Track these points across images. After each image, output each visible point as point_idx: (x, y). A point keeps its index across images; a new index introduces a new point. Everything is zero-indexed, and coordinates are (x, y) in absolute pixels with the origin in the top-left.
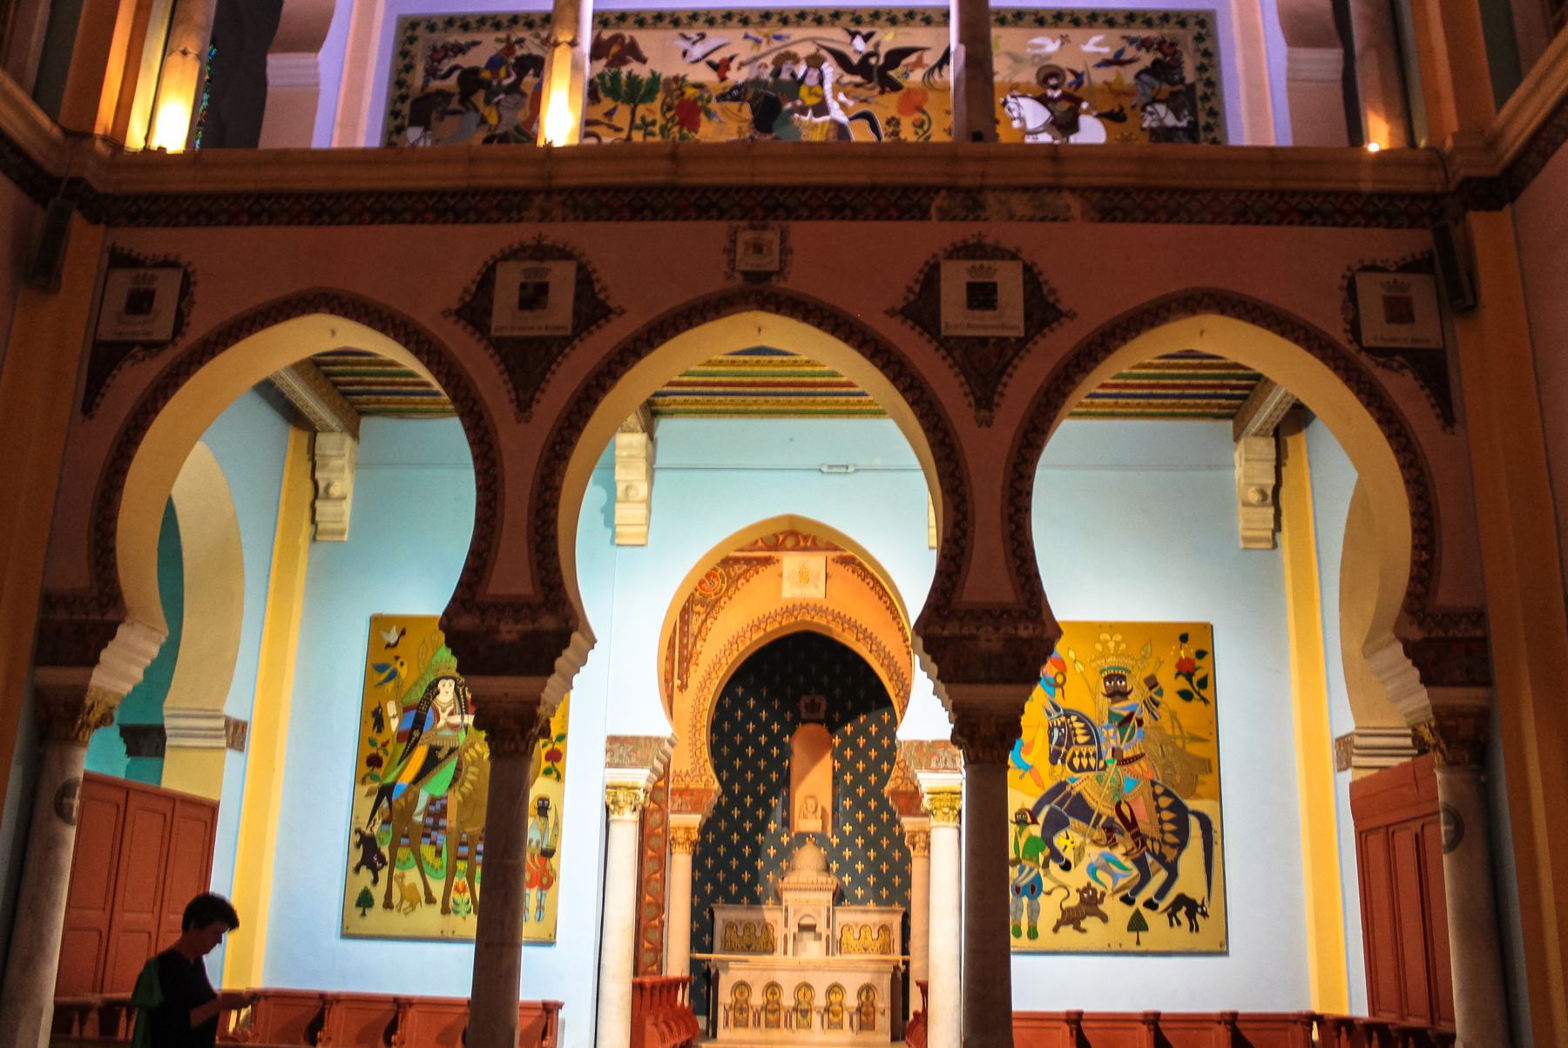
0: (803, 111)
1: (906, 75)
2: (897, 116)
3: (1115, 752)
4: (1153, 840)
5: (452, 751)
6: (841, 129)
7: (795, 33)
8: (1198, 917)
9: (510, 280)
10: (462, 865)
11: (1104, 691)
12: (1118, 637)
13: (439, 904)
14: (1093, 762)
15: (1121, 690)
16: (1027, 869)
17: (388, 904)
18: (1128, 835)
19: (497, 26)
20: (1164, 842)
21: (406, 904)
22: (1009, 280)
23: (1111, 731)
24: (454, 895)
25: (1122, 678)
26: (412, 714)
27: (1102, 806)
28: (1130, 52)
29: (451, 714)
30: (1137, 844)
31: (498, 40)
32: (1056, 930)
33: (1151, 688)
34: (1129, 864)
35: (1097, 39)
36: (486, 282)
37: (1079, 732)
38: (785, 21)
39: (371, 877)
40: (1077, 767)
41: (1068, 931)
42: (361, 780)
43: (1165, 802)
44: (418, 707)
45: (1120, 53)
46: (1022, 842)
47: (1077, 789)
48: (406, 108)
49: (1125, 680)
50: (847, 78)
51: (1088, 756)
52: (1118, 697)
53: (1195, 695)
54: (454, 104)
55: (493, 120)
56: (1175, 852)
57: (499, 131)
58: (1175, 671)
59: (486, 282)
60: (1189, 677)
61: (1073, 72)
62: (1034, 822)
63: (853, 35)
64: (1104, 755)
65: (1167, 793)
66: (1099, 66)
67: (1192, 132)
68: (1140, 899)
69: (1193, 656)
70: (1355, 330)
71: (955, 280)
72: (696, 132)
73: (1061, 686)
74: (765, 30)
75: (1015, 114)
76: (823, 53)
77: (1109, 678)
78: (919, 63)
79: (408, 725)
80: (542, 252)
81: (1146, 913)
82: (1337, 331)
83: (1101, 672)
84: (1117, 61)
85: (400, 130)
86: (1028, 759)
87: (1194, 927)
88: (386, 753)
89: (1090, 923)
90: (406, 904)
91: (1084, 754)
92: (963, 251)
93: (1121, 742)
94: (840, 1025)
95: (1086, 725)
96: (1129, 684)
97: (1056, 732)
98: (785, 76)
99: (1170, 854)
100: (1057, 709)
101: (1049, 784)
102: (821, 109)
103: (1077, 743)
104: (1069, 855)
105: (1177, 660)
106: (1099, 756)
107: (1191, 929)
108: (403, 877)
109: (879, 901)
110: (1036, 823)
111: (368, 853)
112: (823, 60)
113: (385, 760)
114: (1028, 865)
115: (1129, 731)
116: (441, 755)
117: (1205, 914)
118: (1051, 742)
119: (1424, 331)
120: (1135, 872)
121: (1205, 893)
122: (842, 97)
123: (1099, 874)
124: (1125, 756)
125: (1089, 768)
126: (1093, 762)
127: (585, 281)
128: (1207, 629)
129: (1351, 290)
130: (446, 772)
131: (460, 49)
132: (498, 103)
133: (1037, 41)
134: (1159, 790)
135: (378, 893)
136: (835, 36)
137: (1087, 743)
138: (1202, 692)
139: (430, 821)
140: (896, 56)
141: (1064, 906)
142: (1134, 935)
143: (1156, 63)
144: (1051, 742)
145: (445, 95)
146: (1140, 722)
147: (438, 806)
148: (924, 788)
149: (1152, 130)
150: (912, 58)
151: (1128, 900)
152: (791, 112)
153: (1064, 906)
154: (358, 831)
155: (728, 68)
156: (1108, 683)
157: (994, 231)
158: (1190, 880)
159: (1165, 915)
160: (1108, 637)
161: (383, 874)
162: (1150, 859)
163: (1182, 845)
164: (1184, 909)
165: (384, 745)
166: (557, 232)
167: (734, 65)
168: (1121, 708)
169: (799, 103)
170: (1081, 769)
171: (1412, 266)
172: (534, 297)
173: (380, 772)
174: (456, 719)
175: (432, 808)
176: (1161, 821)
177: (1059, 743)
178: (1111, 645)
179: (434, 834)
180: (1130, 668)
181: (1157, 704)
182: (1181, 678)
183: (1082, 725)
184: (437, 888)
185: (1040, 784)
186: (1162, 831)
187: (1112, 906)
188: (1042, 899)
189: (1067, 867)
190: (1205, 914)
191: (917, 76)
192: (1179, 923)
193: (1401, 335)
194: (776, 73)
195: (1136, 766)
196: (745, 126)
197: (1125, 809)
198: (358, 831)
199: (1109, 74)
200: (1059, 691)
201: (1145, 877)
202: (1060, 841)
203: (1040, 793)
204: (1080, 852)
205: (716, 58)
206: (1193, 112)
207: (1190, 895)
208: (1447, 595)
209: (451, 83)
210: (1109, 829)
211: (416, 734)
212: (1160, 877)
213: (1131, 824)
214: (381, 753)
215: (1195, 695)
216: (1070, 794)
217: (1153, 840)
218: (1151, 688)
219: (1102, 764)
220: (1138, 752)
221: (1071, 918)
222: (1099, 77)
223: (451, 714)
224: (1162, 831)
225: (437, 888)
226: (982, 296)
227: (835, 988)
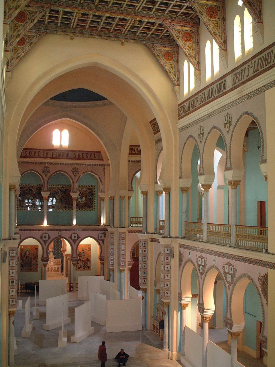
9: (44, 236)
27: (82, 259)
36: (42, 236)
59: (42, 236)
60: (89, 249)
70: (98, 238)
71: (73, 235)
78: (68, 191)
80: (46, 233)
82: (97, 238)
84: (87, 191)
87: (89, 268)
94: (55, 272)
119: (103, 238)
120: (84, 264)
129: (98, 235)
150: (67, 191)
151: (84, 267)
157: (76, 232)
158: (88, 265)
166: (47, 232)
168: (84, 251)
171: (102, 234)
172: (45, 237)
189: (79, 264)
193: (101, 239)
199: (86, 192)
201: (85, 265)
208: (102, 255)
212: (86, 265)
221: (79, 268)
222: (84, 193)
225: (28, 268)
226: (75, 237)
227: (55, 268)
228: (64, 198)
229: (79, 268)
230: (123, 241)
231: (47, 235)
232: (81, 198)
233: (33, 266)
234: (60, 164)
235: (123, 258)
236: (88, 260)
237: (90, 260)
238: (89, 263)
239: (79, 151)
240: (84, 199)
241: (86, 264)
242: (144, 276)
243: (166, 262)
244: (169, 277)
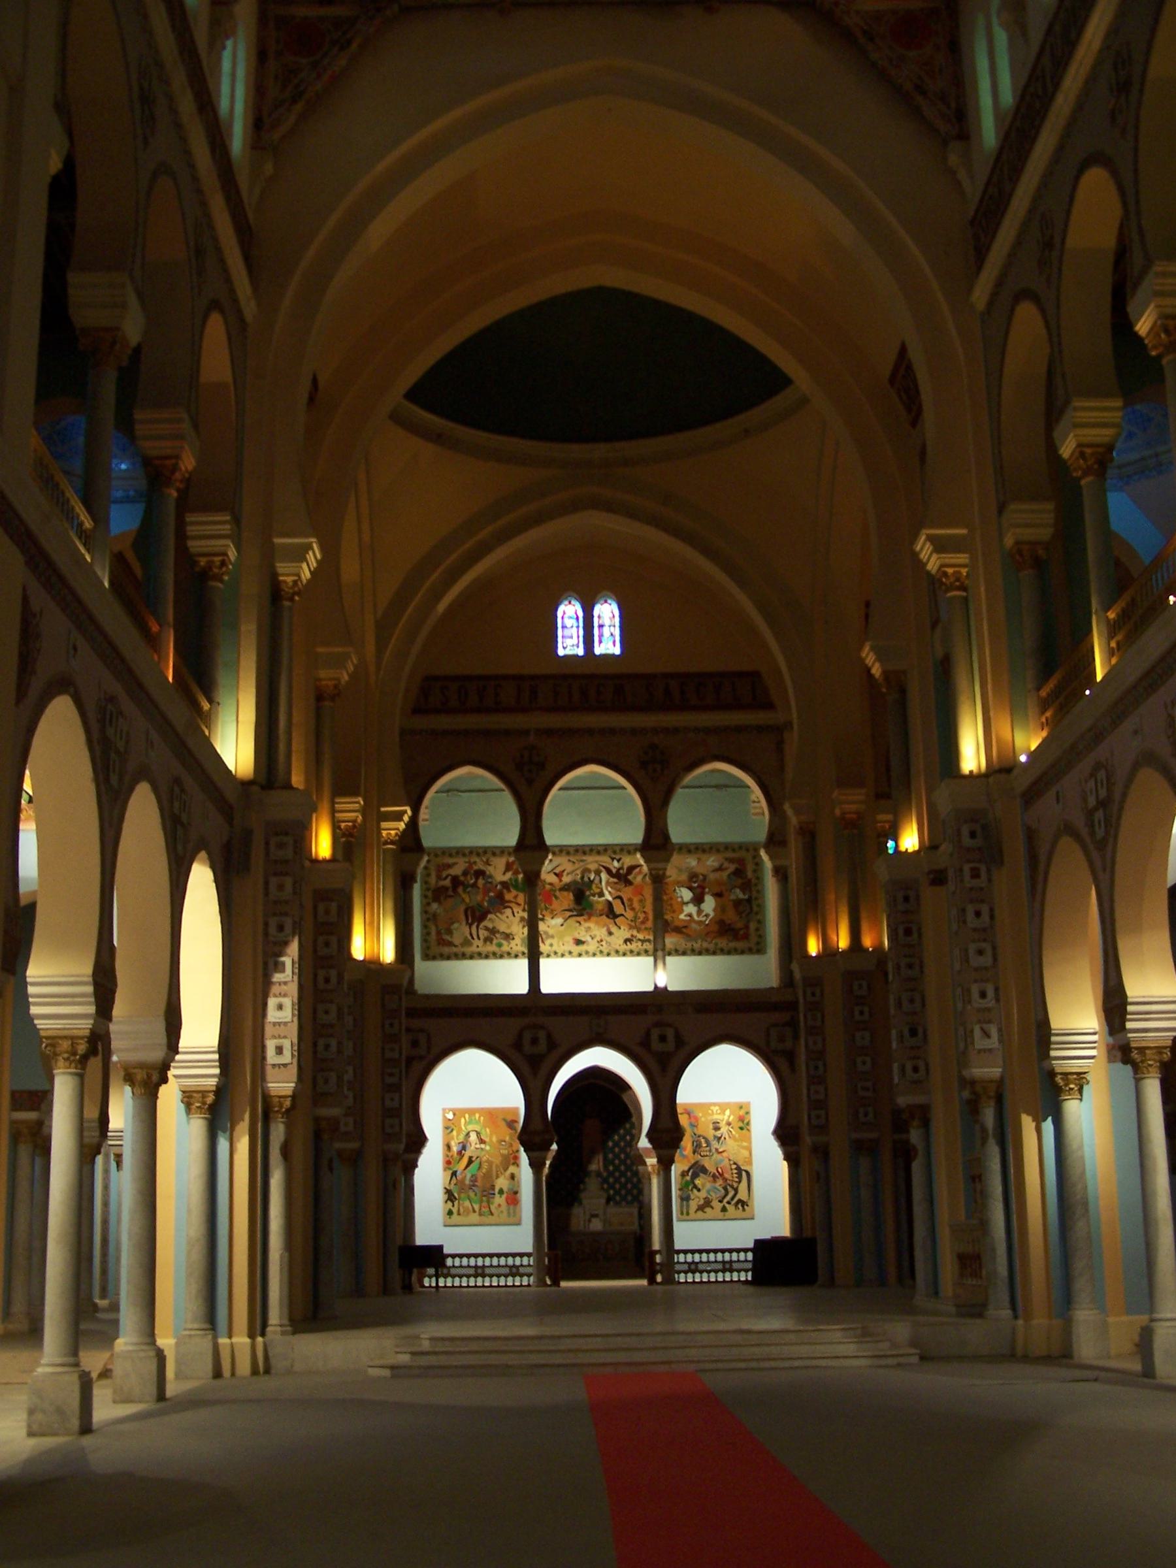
0: (594, 895)
1: (635, 878)
2: (632, 897)
4: (729, 1180)
5: (477, 1158)
6: (609, 904)
7: (589, 858)
8: (746, 1207)
9: (527, 1036)
10: (484, 1198)
13: (477, 1213)
17: (459, 1214)
18: (720, 1178)
19: (464, 855)
21: (465, 1213)
22: (670, 1033)
23: (715, 1142)
24: (483, 1209)
25: (718, 1123)
26: (461, 1145)
27: (711, 1169)
28: (726, 864)
29: (476, 1144)
31: (466, 862)
32: (696, 1212)
34: (721, 1189)
35: (712, 859)
38: (584, 853)
39: (451, 1204)
41: (700, 1213)
42: (445, 1170)
43: (734, 1167)
44: (462, 1142)
45: (722, 865)
48: (430, 894)
50: (612, 880)
54: (450, 893)
55: (467, 900)
57: (471, 905)
61: (703, 875)
63: (613, 859)
65: (735, 1163)
66: (713, 871)
67: (749, 901)
68: (725, 1200)
71: (655, 1034)
72: (551, 905)
74: (578, 858)
75: (679, 895)
76: (602, 868)
78: (640, 872)
79: (460, 1149)
81: (727, 1205)
84: (720, 869)
85: (428, 904)
86: (685, 1153)
87: (744, 1210)
88: (453, 1159)
89: (708, 1210)
90: (465, 1213)
92: (657, 1024)
96: (720, 1125)
98: (586, 879)
99: (735, 1185)
100: (695, 1135)
101: (693, 1162)
102: (601, 894)
104: (700, 1187)
106: (710, 1151)
108: (463, 1203)
109: (627, 1203)
111: (450, 1196)
112: (601, 872)
113: (453, 1162)
116: (474, 1159)
117: (747, 1205)
120: (723, 1191)
122: (609, 889)
123: (711, 1193)
127: (549, 1036)
128: (748, 1104)
130: (474, 1166)
131: (449, 866)
132: (469, 892)
133: (688, 860)
134: (732, 1162)
135: (455, 1210)
136: (605, 859)
139: (471, 1183)
140: (631, 869)
142: (723, 1213)
143: (737, 869)
145: (446, 889)
146: (725, 1138)
147: (474, 1178)
148: (648, 1164)
149: (733, 901)
151: (721, 1201)
152: (589, 896)
154: (445, 1188)
155: (562, 876)
158: (742, 1194)
159: (734, 1207)
161: (456, 1203)
162: (728, 1187)
163: (740, 1182)
165: (452, 1156)
167: (565, 873)
168: (718, 1134)
169: (592, 892)
172: (535, 1041)
173: (451, 1166)
174: (478, 1146)
175: (472, 1179)
176: (732, 1174)
179: (473, 1188)
184: (476, 1207)
185: (689, 1161)
186: (733, 1177)
187: (715, 1203)
188: (691, 1202)
189: (699, 1190)
190: (747, 1205)
191: (639, 878)
192: (739, 1209)
194: (582, 878)
196: (571, 903)
197: (720, 1170)
198: (445, 1188)
199: (717, 875)
201: (727, 1193)
202: (697, 1182)
203: (690, 1165)
204: (703, 1185)
205: (557, 871)
206: (751, 891)
207: (742, 1199)
209: (447, 883)
210: (714, 1176)
211: (463, 1152)
212: (732, 1193)
213: (721, 1175)
214: (451, 1160)
221: (701, 1208)
222: (712, 876)
223: (476, 1144)
225: (476, 1207)
226: (663, 1039)
228: (623, 903)
229: (701, 1208)
230: (862, 1013)
231: (542, 1035)
232: (698, 900)
233: (499, 1200)
234: (590, 732)
235: (866, 1089)
236: (739, 1169)
237: (748, 1174)
238: (743, 1186)
239: (667, 676)
240: (709, 904)
242: (912, 1048)
243: (971, 889)
244: (986, 960)
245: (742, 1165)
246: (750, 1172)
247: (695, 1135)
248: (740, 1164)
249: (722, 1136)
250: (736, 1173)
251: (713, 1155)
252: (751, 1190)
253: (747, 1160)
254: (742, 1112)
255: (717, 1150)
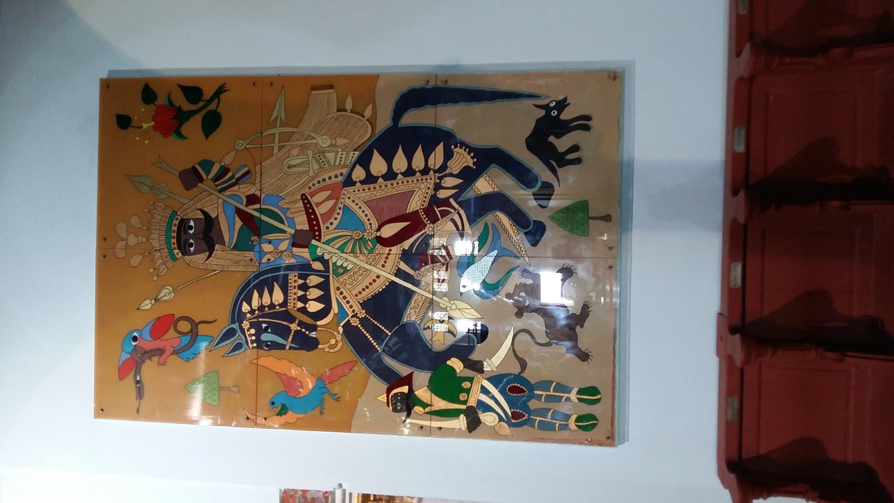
3: (300, 240)
4: (438, 187)
8: (565, 116)
11: (203, 256)
12: (121, 228)
14: (314, 280)
15: (202, 226)
16: (484, 398)
18: (428, 229)
20: (444, 167)
23: (267, 247)
25: (183, 225)
30: (444, 214)
33: (201, 180)
37: (266, 300)
40: (321, 306)
43: (378, 165)
46: (440, 404)
47: (357, 308)
49: (189, 220)
51: (304, 287)
52: (214, 234)
53: (212, 106)
56: (457, 150)
58: (173, 138)
60: (182, 116)
62: (408, 380)
64: (301, 261)
65: (364, 161)
69: (152, 107)
73: (195, 325)
77: (184, 248)
83: (174, 258)
87: (583, 123)
91: (301, 293)
93: (285, 232)
95: (255, 287)
97: (266, 337)
99: (462, 159)
100: (230, 334)
101: (350, 354)
103: (284, 304)
105: (158, 135)
106: (305, 269)
107: (587, 128)
110: (410, 376)
114: (475, 397)
115: (264, 218)
117: (562, 105)
118: (282, 347)
121: (527, 103)
124: (306, 227)
125: (324, 286)
126: (314, 280)
134: (359, 173)
137: (285, 290)
138: (208, 94)
141: (545, 340)
144: (282, 347)
146: (252, 199)
153: (545, 340)
156: (192, 249)
160: (121, 244)
163: (448, 139)
164: (552, 139)
170: (325, 299)
176: (410, 172)
177: (284, 332)
178: (132, 240)
180: (169, 211)
181: (225, 171)
182: (185, 129)
183: (256, 295)
186: (425, 171)
188: (530, 375)
190: (562, 105)
192: (575, 148)
195: (320, 211)
197: (389, 230)
200: (201, 327)
203: (361, 368)
215: (212, 106)
216: (363, 321)
217: (438, 187)
218: (201, 180)
219: (317, 266)
220: (300, 204)
224: (425, 171)
241: (483, 186)
245: (372, 122)
246: (405, 89)
247: (230, 334)
248: (365, 135)
249: (240, 212)
250: (409, 157)
251: (321, 259)
252: (487, 86)
253: (349, 105)
254: (146, 122)
255: (300, 240)
